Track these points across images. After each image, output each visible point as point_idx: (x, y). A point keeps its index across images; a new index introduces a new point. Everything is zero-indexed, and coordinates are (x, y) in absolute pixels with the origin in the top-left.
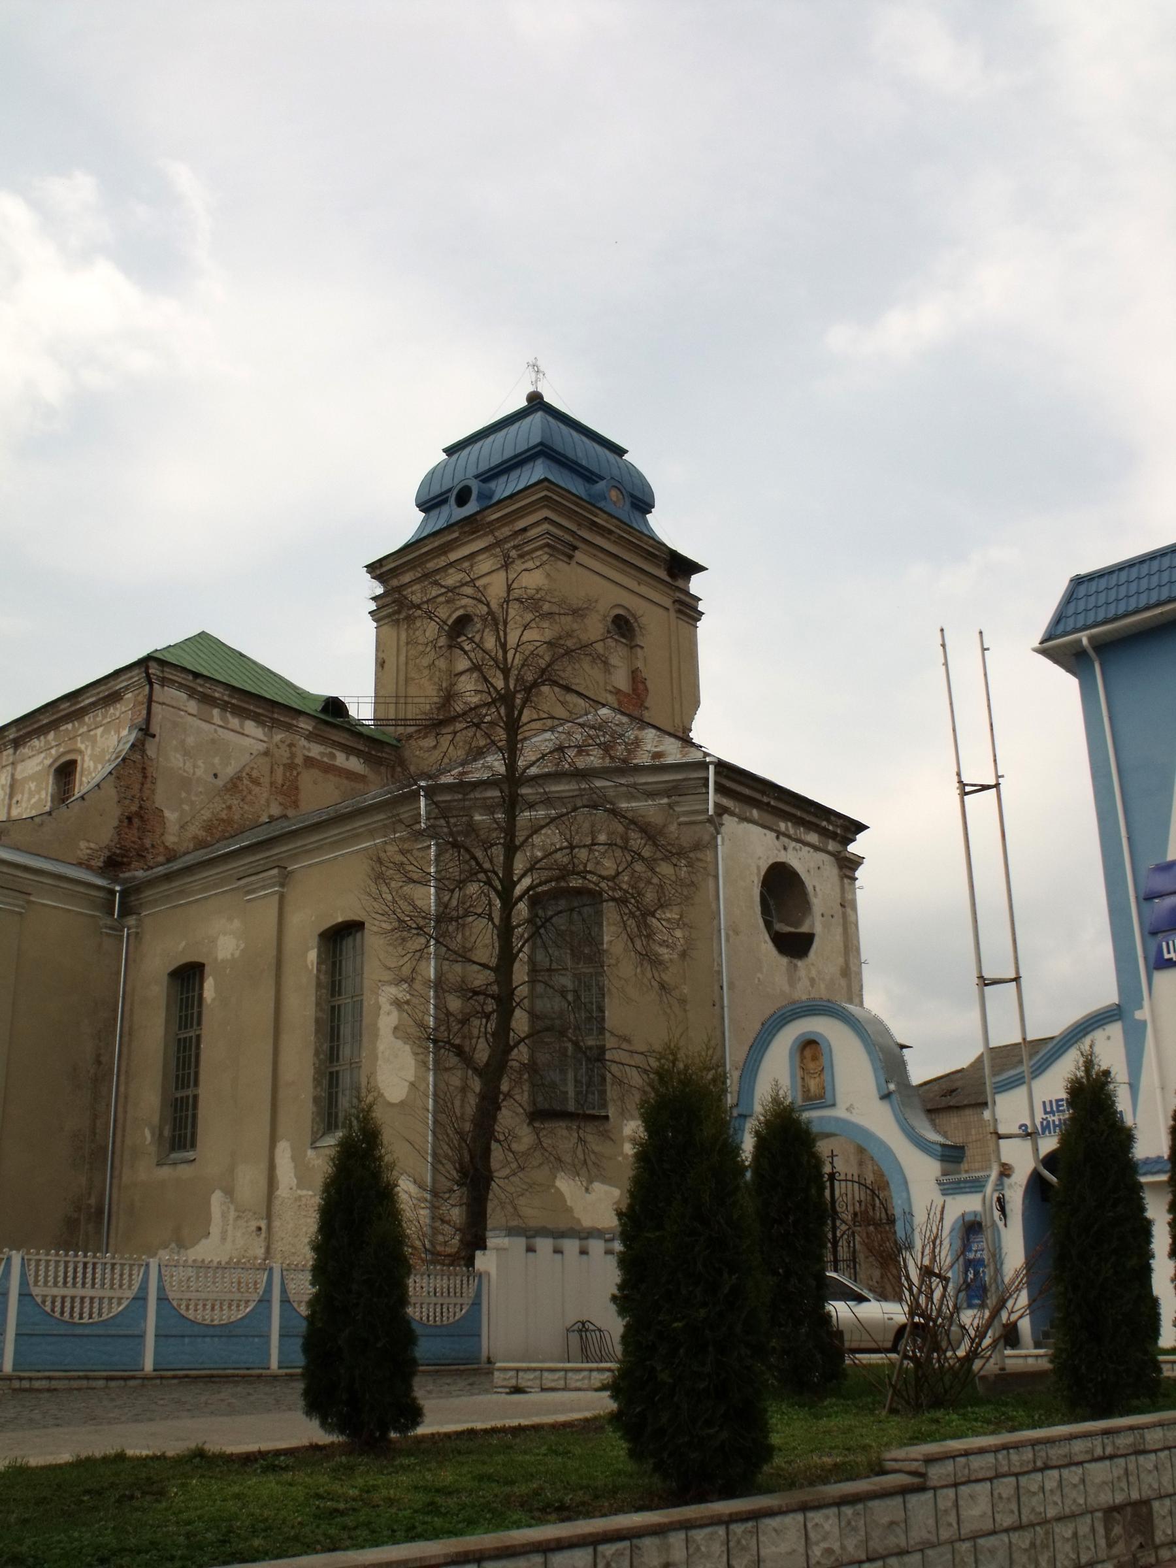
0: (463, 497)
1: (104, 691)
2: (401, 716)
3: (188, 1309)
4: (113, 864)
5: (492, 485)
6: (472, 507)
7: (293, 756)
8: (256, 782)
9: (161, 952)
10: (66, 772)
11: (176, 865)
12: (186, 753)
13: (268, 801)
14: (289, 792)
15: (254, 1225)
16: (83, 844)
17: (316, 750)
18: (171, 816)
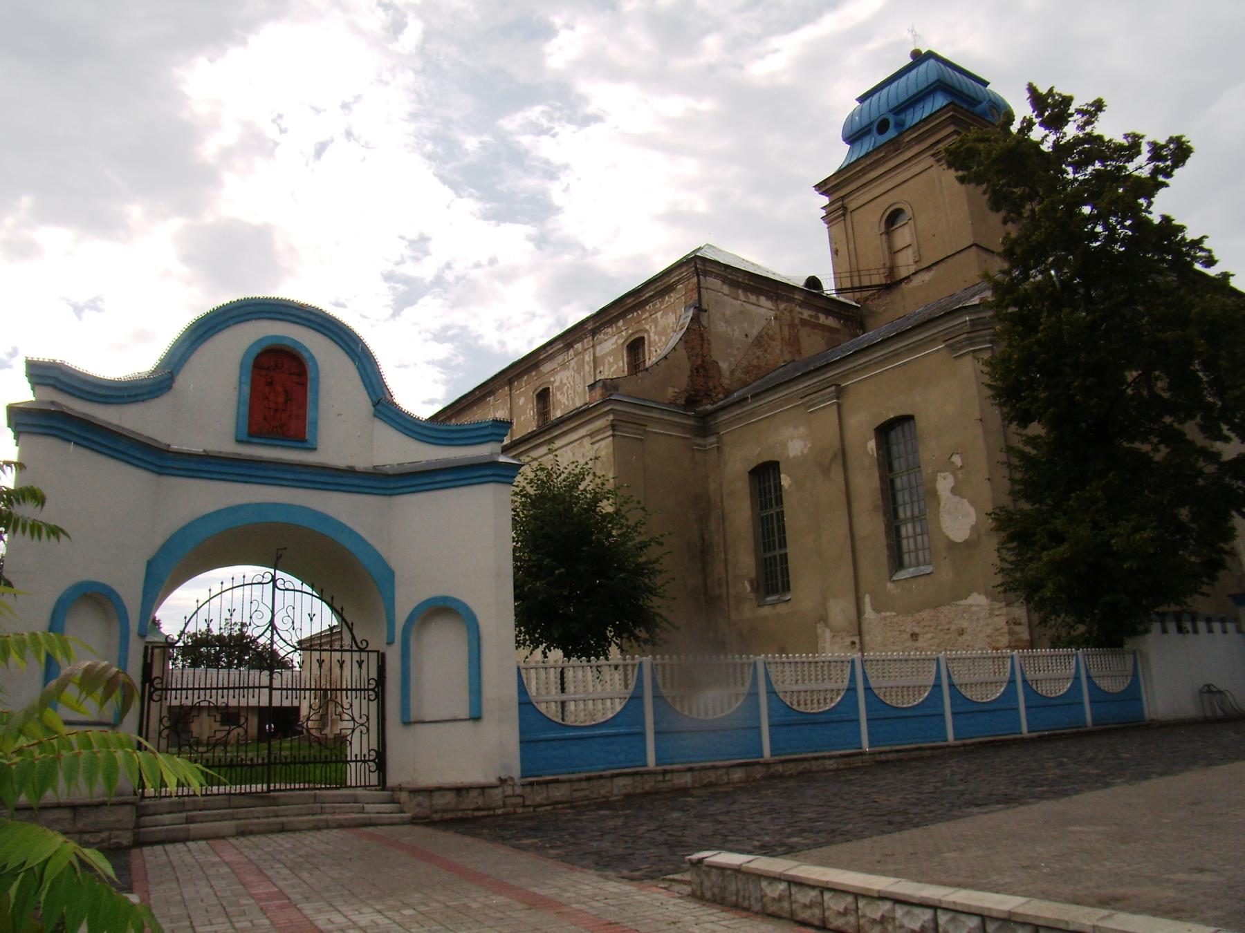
0: (883, 126)
1: (660, 285)
2: (857, 284)
3: (799, 705)
4: (692, 401)
5: (902, 117)
6: (891, 133)
7: (793, 318)
8: (772, 338)
9: (740, 455)
10: (635, 347)
11: (730, 399)
12: (727, 322)
13: (781, 351)
14: (794, 343)
15: (848, 640)
16: (671, 390)
17: (806, 314)
18: (724, 366)
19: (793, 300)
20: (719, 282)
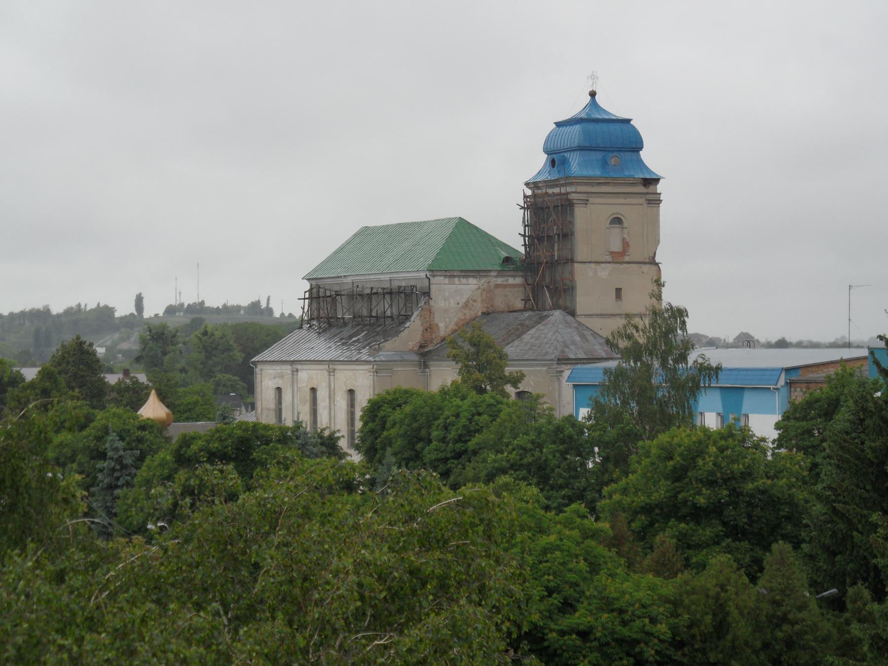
8: (475, 301)
17: (500, 281)
18: (441, 325)
19: (491, 276)
20: (442, 278)
